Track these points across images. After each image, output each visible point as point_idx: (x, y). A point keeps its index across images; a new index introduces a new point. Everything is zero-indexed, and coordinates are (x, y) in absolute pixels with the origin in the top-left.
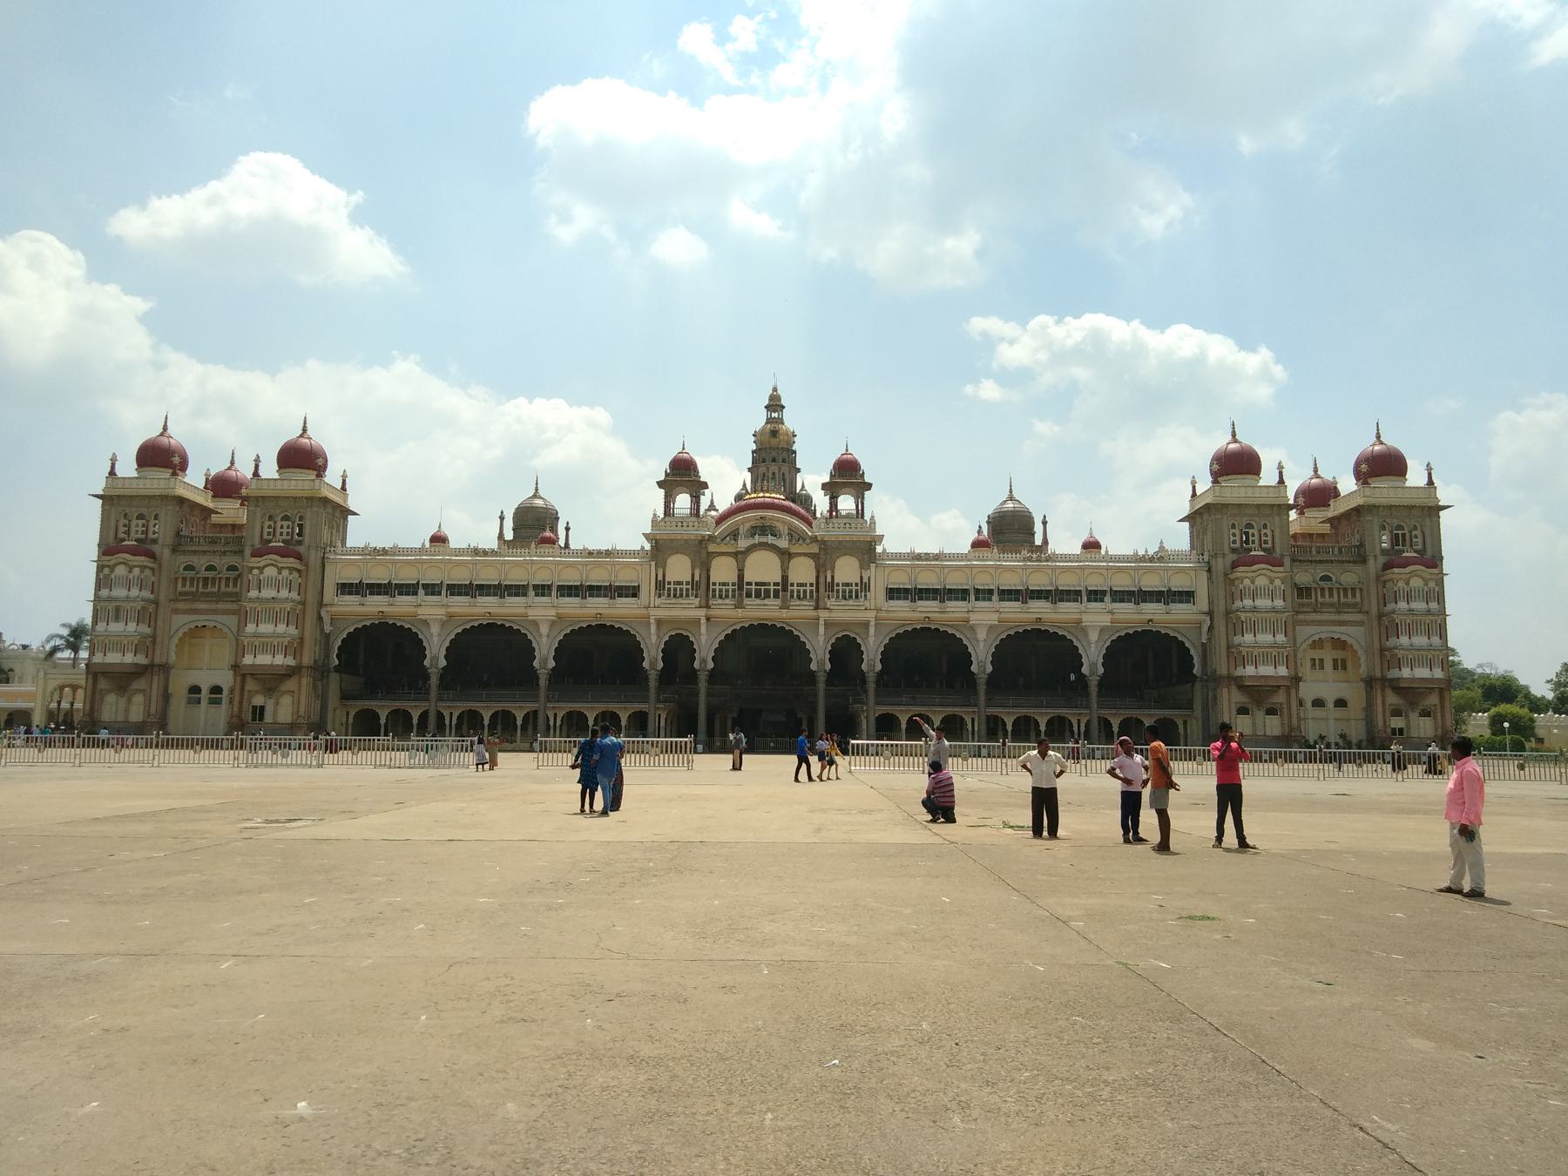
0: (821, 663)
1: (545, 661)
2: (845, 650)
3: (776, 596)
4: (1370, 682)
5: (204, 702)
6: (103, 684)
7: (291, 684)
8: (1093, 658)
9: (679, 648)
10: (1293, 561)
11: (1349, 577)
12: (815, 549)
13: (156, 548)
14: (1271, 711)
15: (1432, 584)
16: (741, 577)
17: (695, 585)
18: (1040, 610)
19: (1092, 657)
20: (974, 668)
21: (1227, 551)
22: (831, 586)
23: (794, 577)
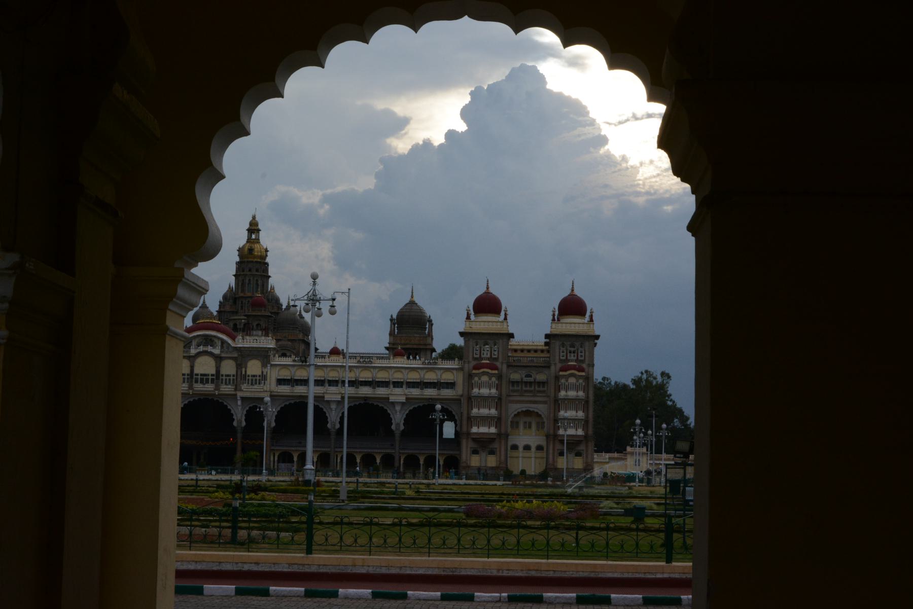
2: (254, 415)
4: (548, 436)
10: (509, 366)
11: (541, 377)
12: (236, 355)
14: (492, 452)
15: (581, 381)
18: (365, 391)
19: (398, 419)
20: (329, 426)
21: (471, 359)
22: (245, 377)
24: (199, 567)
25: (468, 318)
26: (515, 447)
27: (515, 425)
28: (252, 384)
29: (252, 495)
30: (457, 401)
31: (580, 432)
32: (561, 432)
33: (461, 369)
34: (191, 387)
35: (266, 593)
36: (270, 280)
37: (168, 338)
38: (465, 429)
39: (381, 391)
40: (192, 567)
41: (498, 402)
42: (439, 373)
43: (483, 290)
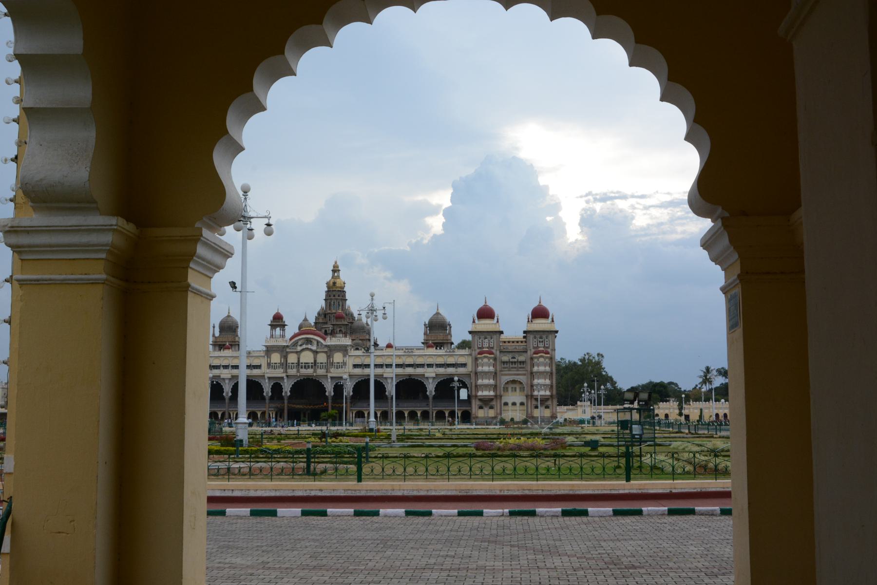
0: (330, 392)
1: (227, 393)
2: (339, 389)
4: (527, 396)
9: (277, 388)
10: (500, 352)
11: (521, 358)
16: (299, 361)
17: (281, 364)
18: (410, 371)
19: (431, 388)
23: (319, 361)
24: (278, 494)
25: (474, 322)
26: (506, 404)
27: (506, 389)
29: (334, 439)
30: (469, 375)
31: (548, 393)
32: (536, 393)
33: (471, 355)
34: (298, 371)
35: (324, 514)
36: (348, 303)
37: (190, 295)
38: (474, 393)
39: (419, 371)
40: (273, 494)
41: (495, 375)
42: (456, 357)
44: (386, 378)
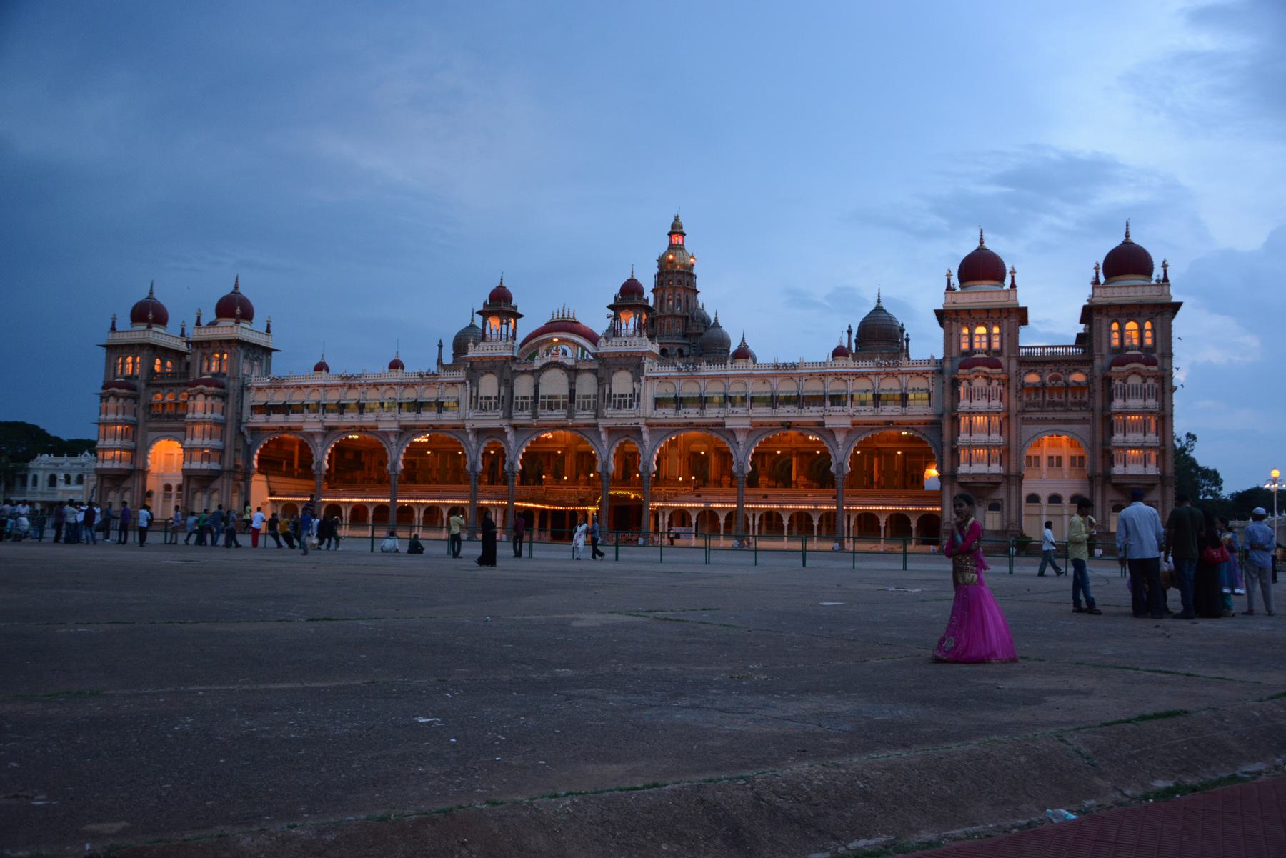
3: (564, 407)
4: (1091, 479)
5: (174, 497)
6: (107, 484)
7: (217, 484)
8: (840, 458)
11: (1078, 377)
12: (596, 366)
13: (137, 383)
14: (995, 506)
15: (1150, 381)
18: (786, 413)
21: (955, 353)
26: (1033, 499)
28: (619, 408)
31: (1152, 470)
34: (535, 415)
36: (699, 297)
42: (904, 379)
43: (977, 245)
44: (732, 432)
